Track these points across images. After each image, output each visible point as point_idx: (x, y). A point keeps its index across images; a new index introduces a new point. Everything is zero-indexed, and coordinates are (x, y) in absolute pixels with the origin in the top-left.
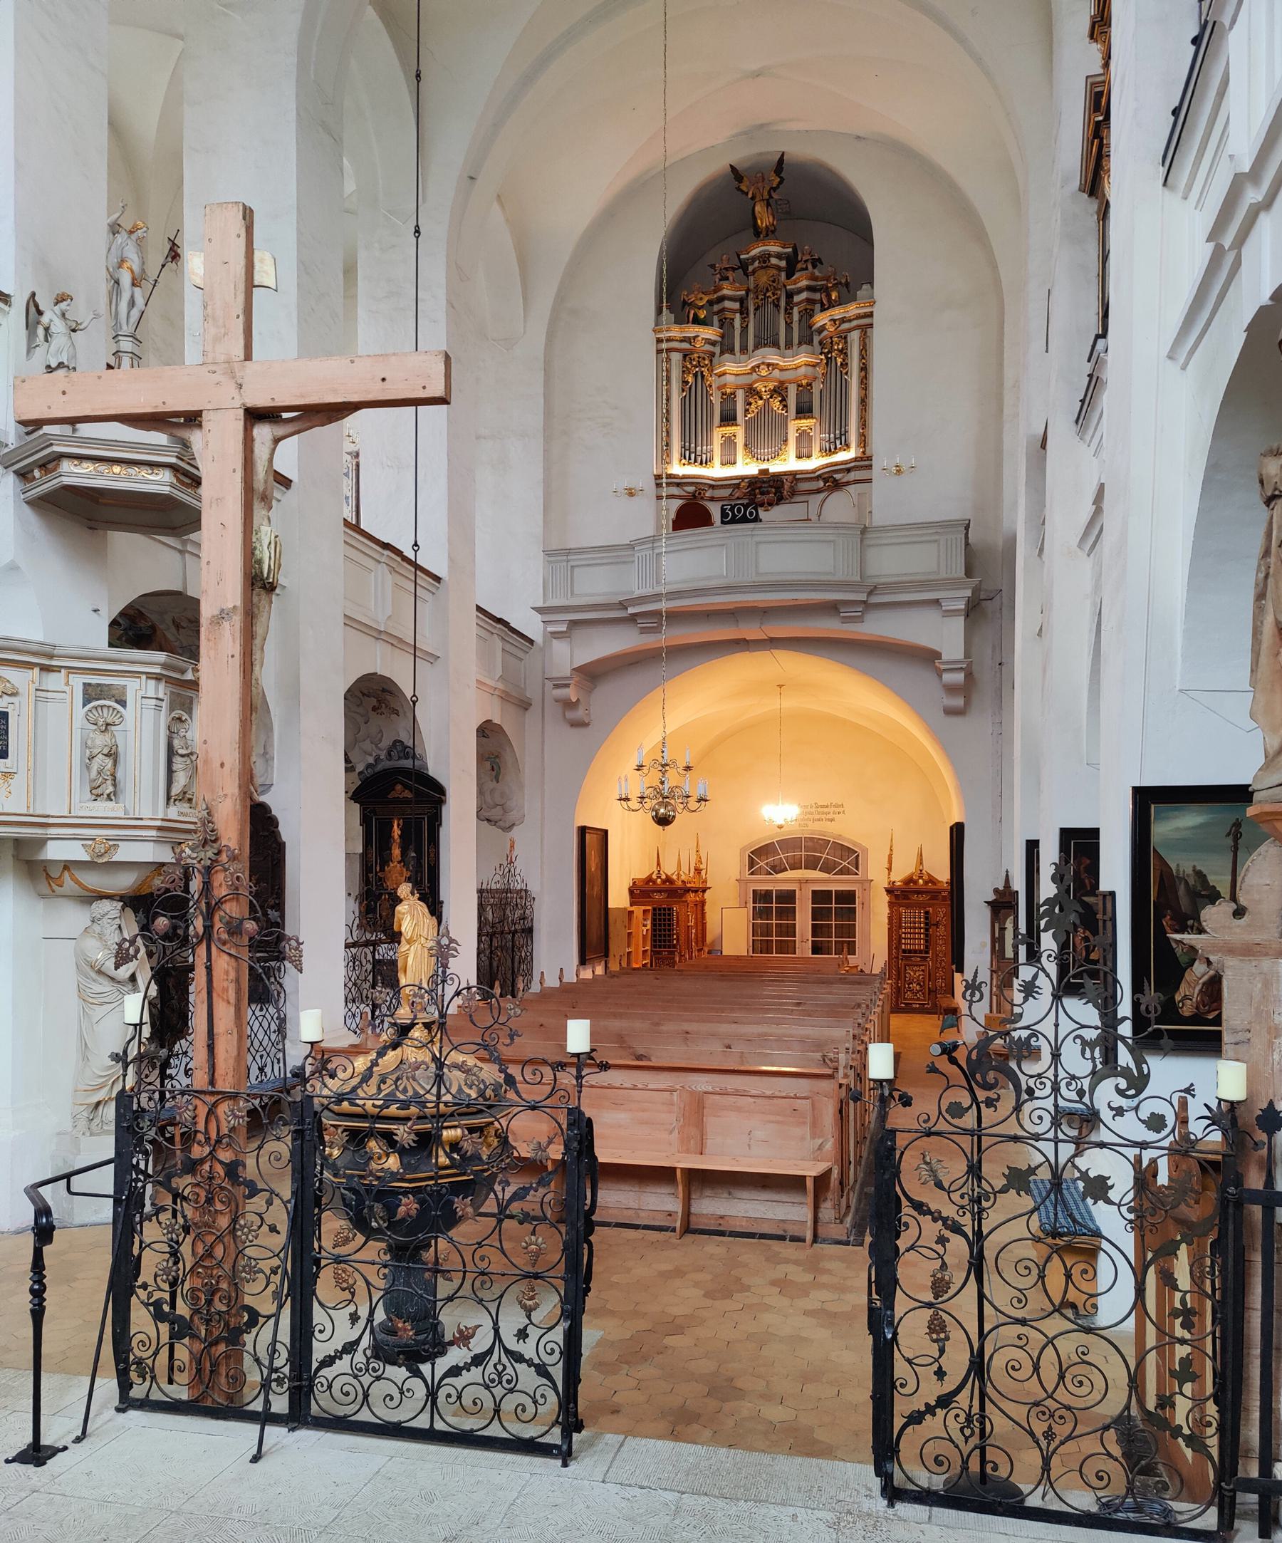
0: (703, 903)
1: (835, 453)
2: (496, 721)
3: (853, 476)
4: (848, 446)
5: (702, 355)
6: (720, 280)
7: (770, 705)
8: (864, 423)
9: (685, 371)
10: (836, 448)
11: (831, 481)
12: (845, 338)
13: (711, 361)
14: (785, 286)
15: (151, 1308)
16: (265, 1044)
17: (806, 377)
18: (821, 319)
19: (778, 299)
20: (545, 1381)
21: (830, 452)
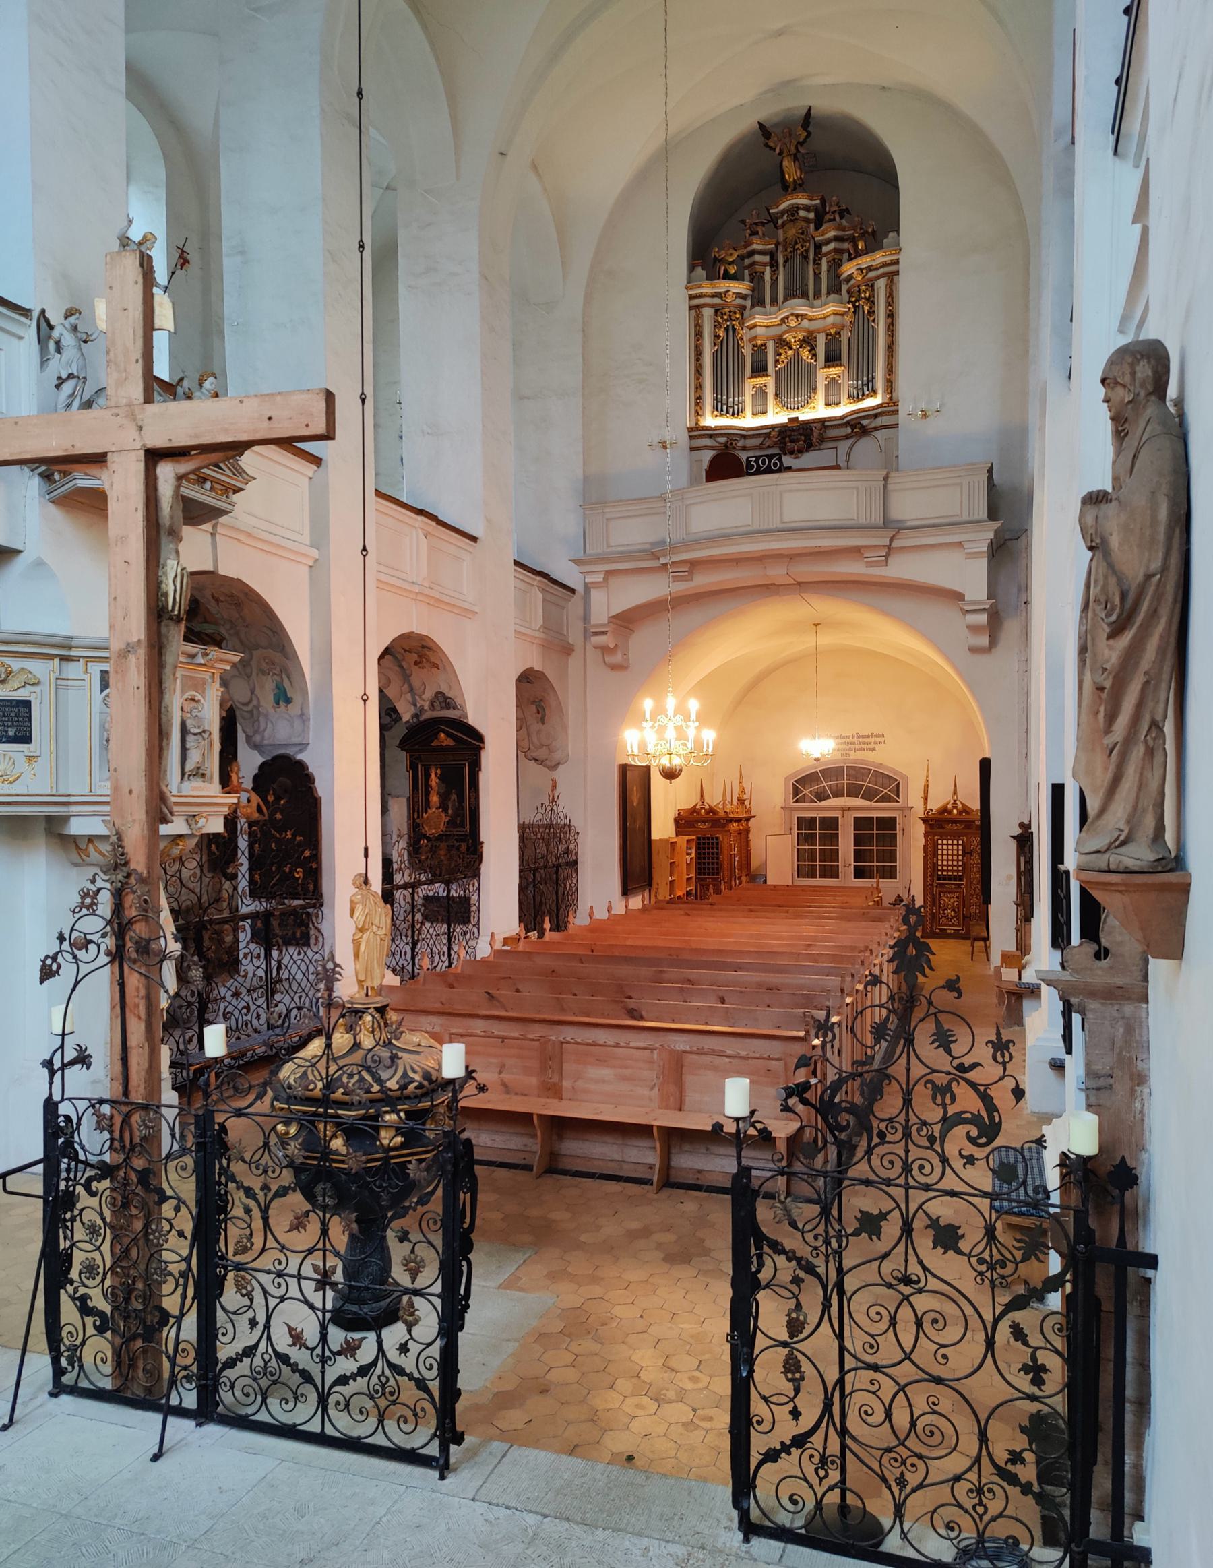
0: (747, 831)
1: (862, 399)
2: (536, 669)
3: (879, 421)
4: (875, 392)
6: (750, 235)
7: (806, 642)
8: (890, 369)
9: (717, 325)
10: (863, 395)
11: (858, 427)
12: (872, 286)
13: (742, 314)
14: (813, 238)
15: (78, 1303)
16: (303, 985)
17: (834, 325)
18: (849, 268)
19: (807, 251)
20: (426, 1396)
21: (857, 398)
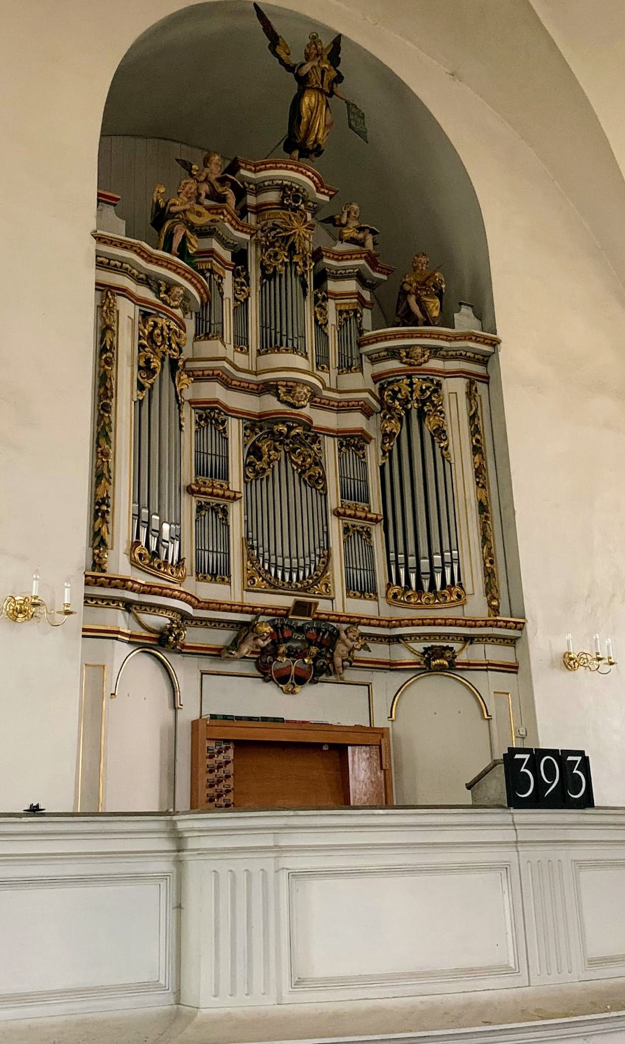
5: (173, 325)
14: (317, 255)
